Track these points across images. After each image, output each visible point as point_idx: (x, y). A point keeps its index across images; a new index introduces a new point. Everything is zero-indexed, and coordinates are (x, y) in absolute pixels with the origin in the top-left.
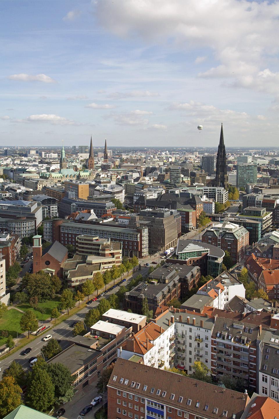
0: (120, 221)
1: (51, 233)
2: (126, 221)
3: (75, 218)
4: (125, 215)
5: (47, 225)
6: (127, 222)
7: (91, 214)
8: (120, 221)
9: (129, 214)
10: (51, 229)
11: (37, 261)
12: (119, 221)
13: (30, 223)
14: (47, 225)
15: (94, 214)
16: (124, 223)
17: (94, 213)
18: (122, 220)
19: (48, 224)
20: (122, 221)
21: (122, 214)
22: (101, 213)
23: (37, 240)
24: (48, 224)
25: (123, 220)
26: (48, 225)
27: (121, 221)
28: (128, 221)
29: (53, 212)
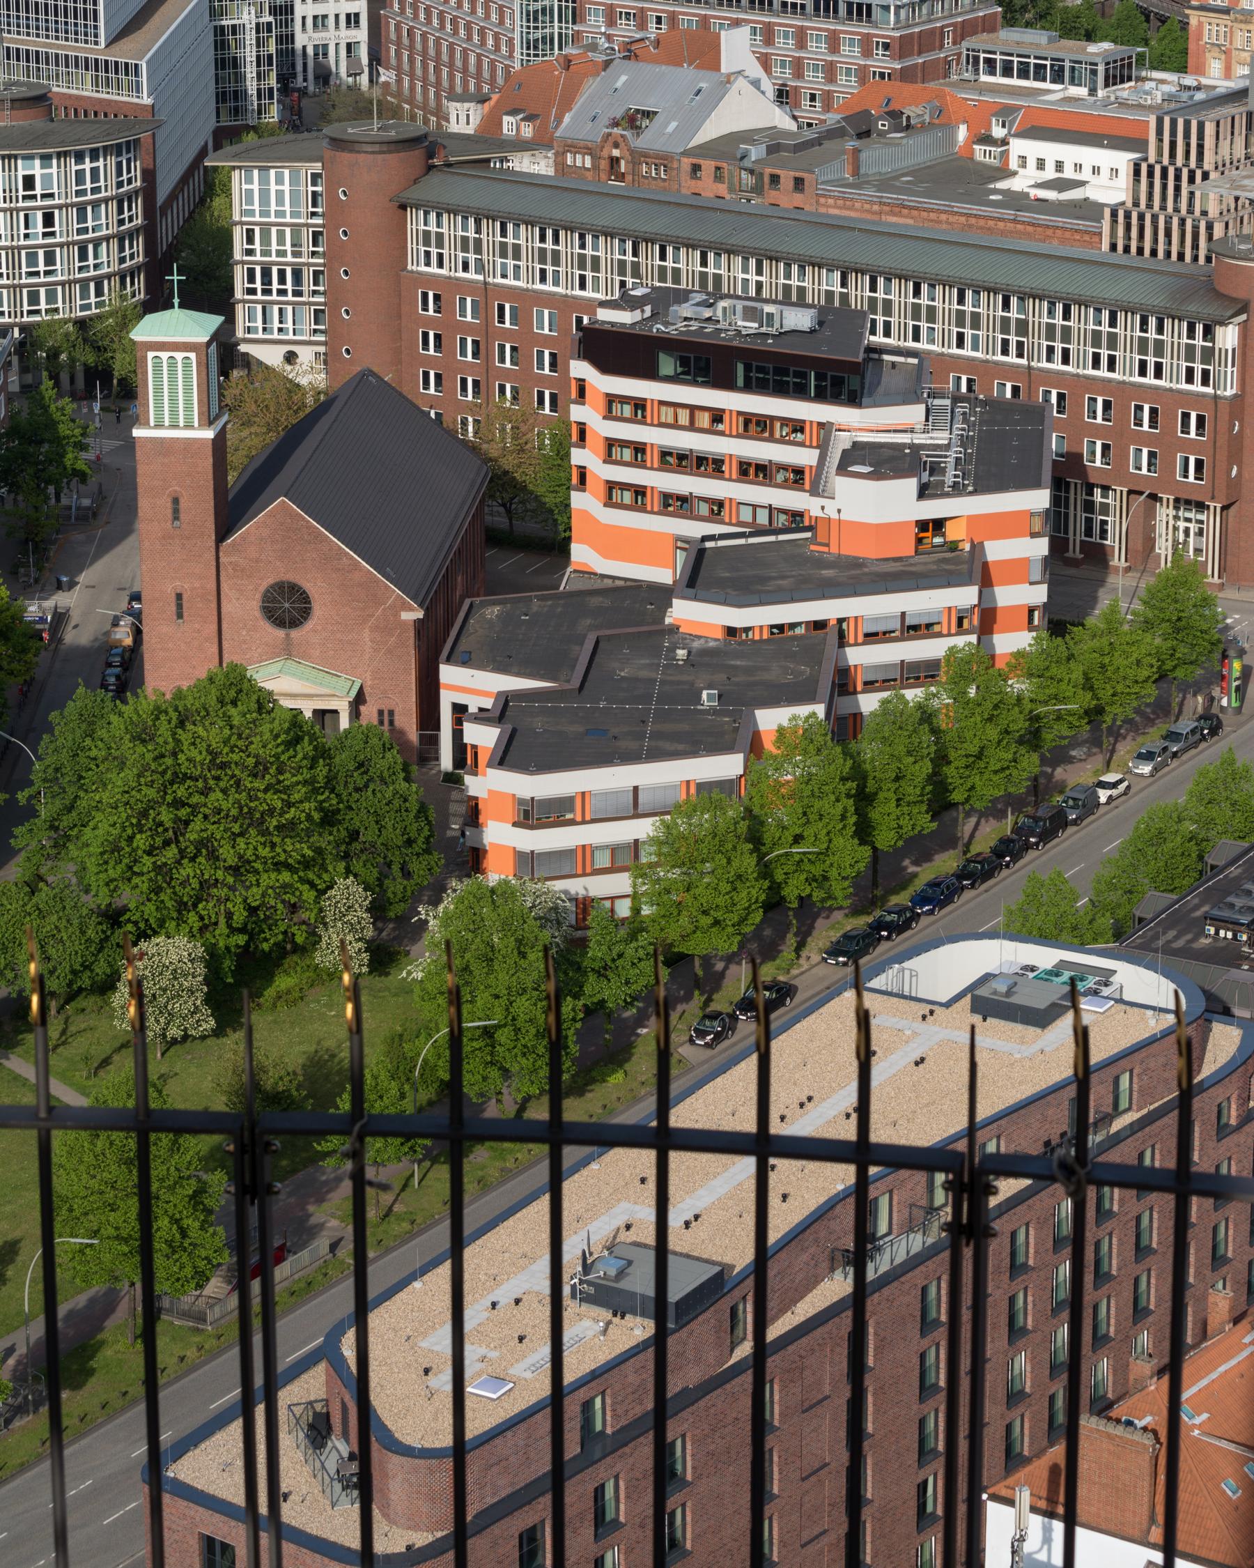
0: (1032, 163)
1: (308, 276)
2: (1096, 170)
3: (559, 120)
4: (1093, 91)
5: (264, 194)
6: (1115, 172)
7: (729, 80)
8: (1032, 163)
9: (1125, 90)
10: (306, 237)
11: (185, 586)
12: (1023, 160)
13: (94, 171)
14: (264, 194)
15: (756, 84)
16: (1082, 184)
17: (756, 71)
18: (1052, 151)
19: (280, 181)
20: (1059, 166)
21: (1058, 77)
22: (830, 71)
23: (179, 356)
24: (280, 181)
25: (1070, 153)
26: (280, 194)
27: (1041, 164)
28: (1122, 160)
29: (319, 37)
